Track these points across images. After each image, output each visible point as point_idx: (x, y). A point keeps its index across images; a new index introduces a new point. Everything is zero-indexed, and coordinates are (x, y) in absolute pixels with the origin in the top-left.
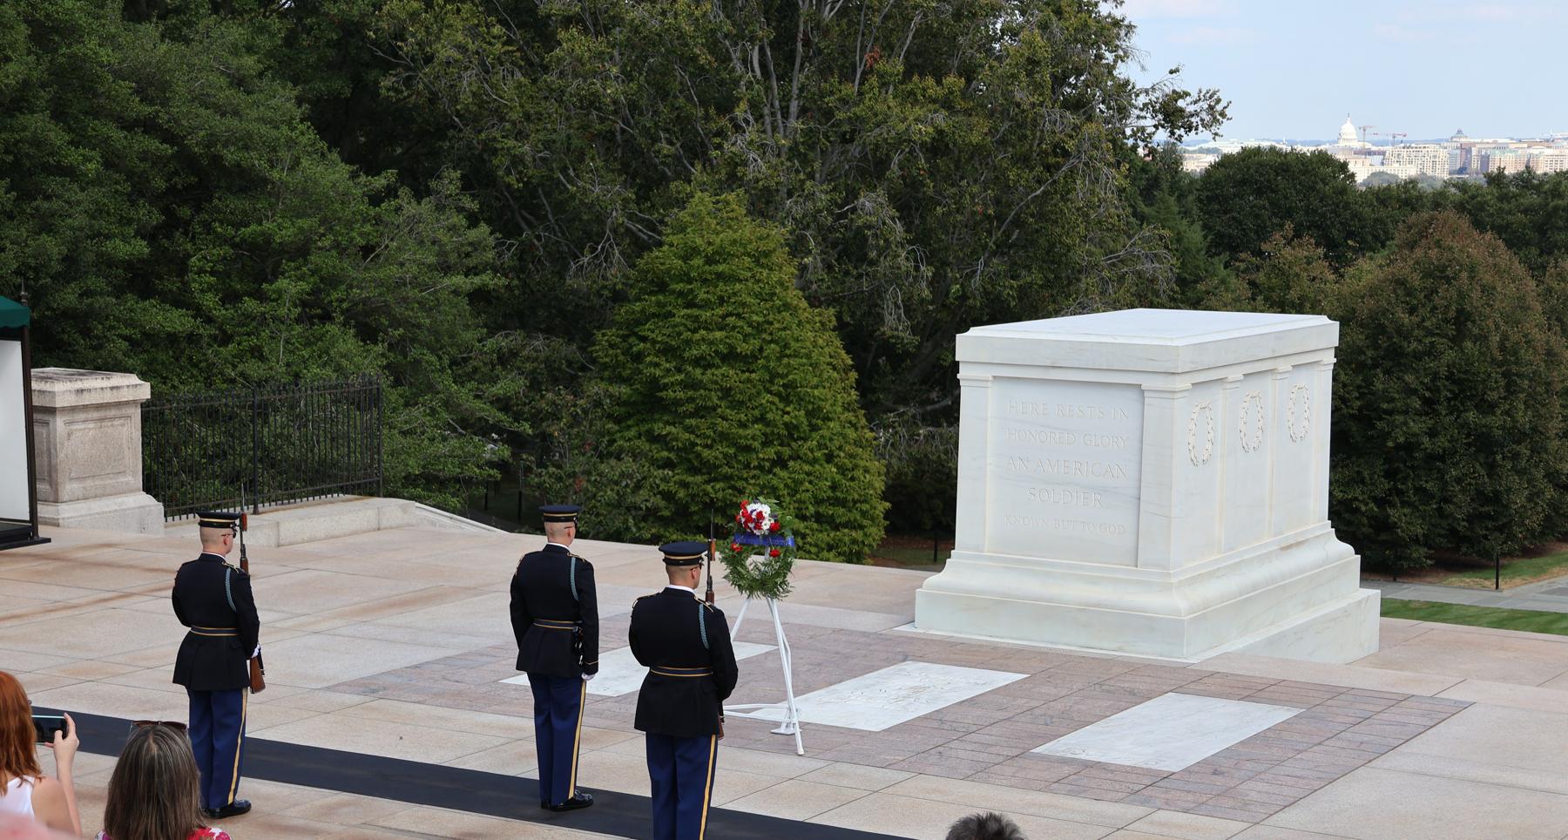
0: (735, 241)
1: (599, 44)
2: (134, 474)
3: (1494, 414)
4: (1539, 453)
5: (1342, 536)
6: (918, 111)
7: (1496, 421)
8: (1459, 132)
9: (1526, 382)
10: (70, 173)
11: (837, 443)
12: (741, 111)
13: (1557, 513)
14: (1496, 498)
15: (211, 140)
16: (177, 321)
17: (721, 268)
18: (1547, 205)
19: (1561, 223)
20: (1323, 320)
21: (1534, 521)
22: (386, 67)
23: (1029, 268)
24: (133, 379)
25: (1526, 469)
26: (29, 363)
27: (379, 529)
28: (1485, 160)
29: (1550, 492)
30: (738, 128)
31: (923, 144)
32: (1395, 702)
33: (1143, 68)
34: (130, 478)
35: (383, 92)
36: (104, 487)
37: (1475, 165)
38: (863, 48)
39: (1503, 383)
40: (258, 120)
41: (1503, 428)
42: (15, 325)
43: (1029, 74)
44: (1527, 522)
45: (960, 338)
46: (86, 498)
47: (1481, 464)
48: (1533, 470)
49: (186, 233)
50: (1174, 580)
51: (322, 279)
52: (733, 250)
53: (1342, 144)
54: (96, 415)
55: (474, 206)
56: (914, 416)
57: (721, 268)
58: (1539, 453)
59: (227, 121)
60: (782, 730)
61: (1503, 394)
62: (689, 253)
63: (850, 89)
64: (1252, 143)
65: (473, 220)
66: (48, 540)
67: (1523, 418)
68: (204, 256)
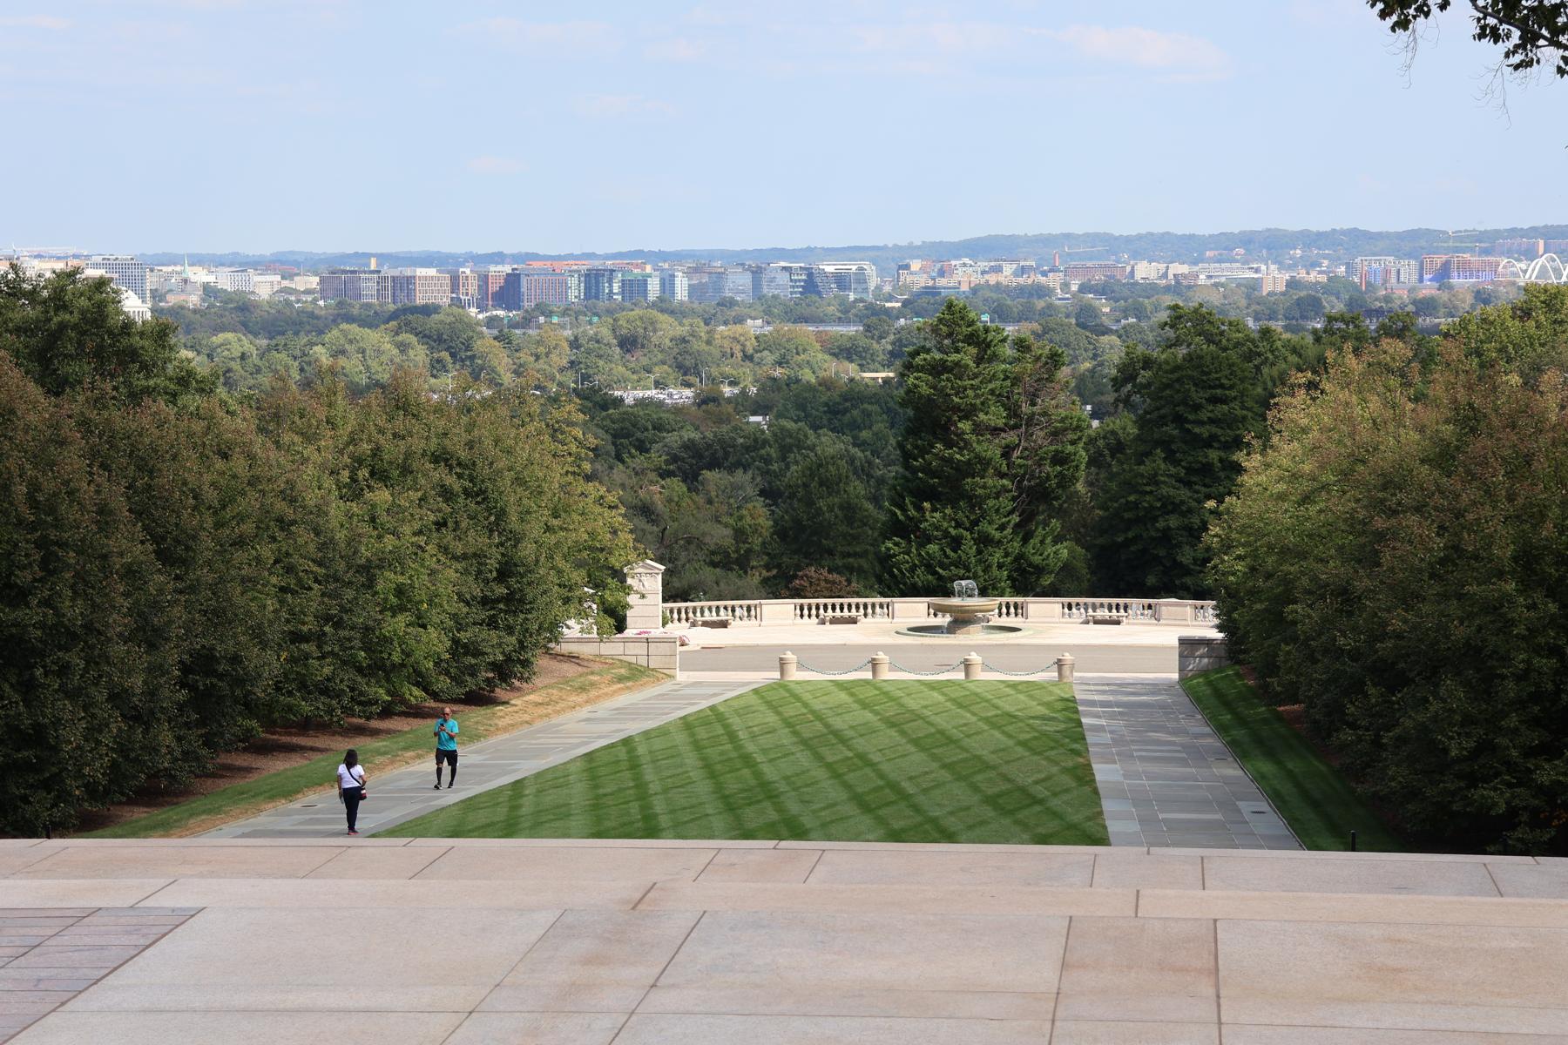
3: (27, 606)
4: (97, 664)
7: (31, 615)
9: (72, 554)
13: (127, 758)
14: (38, 737)
18: (50, 320)
19: (71, 349)
21: (96, 770)
25: (80, 689)
29: (116, 725)
32: (76, 919)
39: (37, 556)
41: (42, 625)
44: (86, 770)
47: (12, 686)
48: (92, 690)
58: (97, 664)
61: (40, 574)
67: (74, 611)
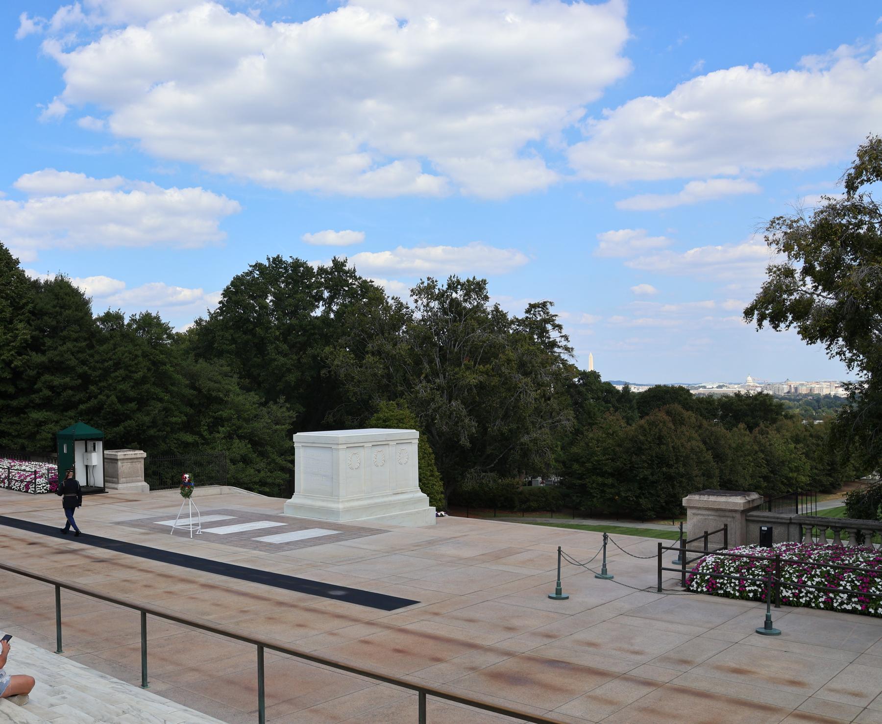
0: (392, 415)
1: (376, 359)
2: (142, 477)
5: (423, 491)
6: (475, 376)
8: (788, 380)
10: (161, 400)
11: (423, 476)
12: (422, 378)
15: (209, 390)
16: (189, 438)
17: (387, 424)
20: (415, 431)
22: (324, 367)
23: (512, 423)
24: (142, 452)
26: (106, 447)
27: (221, 494)
28: (796, 389)
30: (421, 382)
31: (475, 386)
33: (577, 361)
34: (141, 478)
35: (321, 375)
36: (132, 480)
37: (793, 390)
38: (463, 358)
40: (226, 384)
42: (100, 437)
43: (508, 364)
45: (294, 436)
46: (127, 483)
49: (203, 415)
50: (340, 500)
51: (237, 427)
52: (391, 418)
53: (747, 384)
54: (130, 461)
55: (288, 406)
56: (479, 470)
57: (387, 424)
59: (216, 385)
60: (197, 533)
62: (379, 419)
63: (457, 369)
64: (658, 383)
65: (288, 409)
66: (108, 492)
68: (205, 421)
